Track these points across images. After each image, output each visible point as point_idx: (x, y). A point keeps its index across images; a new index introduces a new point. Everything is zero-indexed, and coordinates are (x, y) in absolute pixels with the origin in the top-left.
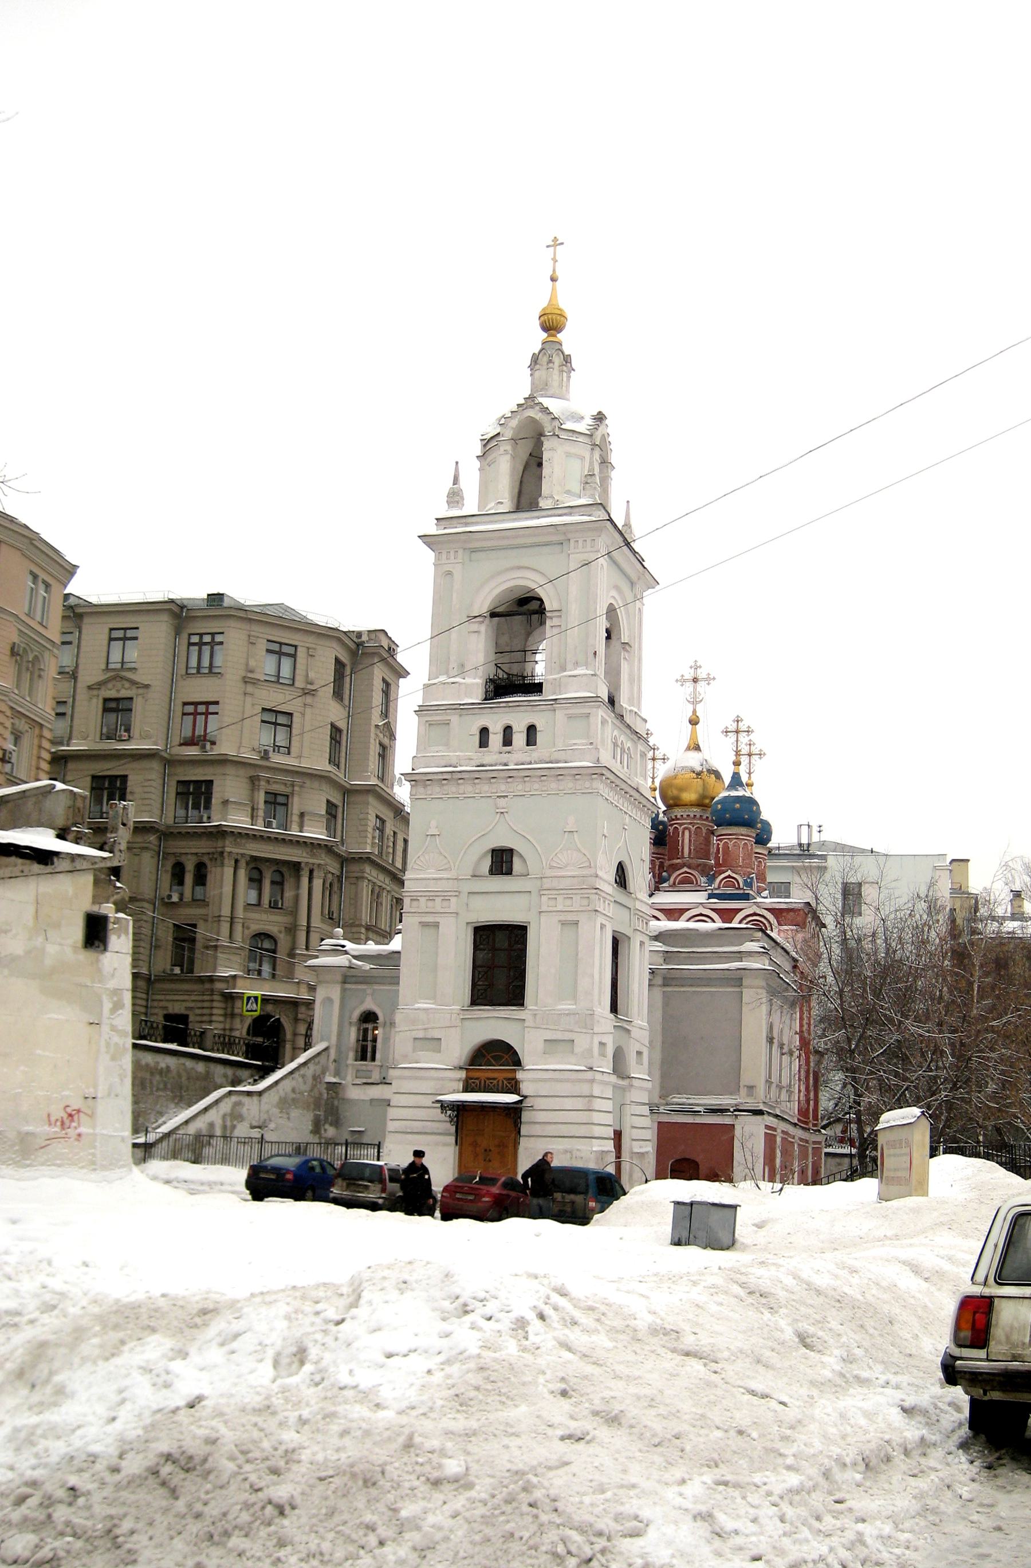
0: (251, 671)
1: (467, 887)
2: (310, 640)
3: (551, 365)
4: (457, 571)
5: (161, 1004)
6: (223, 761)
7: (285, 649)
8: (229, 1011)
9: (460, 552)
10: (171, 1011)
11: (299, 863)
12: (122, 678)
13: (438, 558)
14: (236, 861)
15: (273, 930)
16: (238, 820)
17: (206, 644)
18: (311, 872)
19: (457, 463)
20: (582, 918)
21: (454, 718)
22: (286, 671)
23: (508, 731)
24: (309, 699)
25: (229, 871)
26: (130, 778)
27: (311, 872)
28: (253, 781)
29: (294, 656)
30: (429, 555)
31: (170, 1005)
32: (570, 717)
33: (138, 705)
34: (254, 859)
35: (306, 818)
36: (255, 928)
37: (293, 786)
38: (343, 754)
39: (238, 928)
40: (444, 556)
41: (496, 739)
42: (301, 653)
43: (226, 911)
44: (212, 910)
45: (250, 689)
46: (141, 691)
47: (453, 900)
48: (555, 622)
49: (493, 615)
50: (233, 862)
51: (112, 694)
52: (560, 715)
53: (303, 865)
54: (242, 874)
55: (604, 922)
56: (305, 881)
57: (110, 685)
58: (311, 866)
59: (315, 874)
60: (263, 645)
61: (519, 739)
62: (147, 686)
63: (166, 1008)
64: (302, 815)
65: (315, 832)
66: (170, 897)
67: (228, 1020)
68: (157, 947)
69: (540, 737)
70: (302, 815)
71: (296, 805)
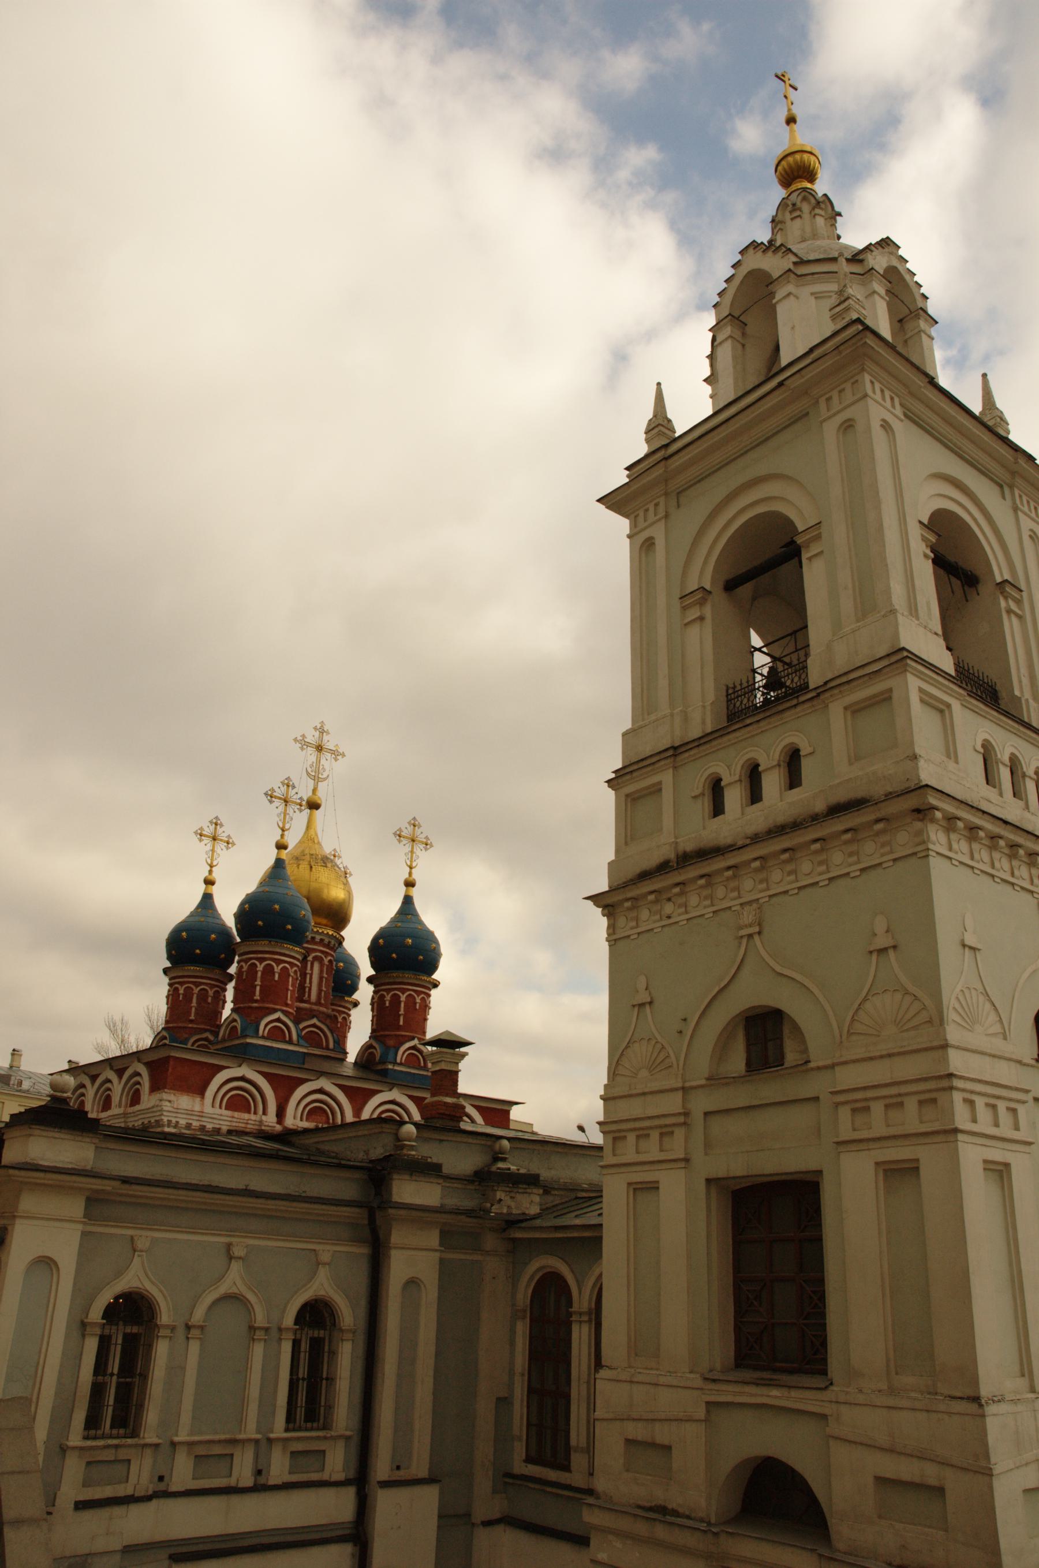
1: (701, 1103)
3: (797, 213)
4: (658, 533)
9: (662, 500)
13: (634, 525)
19: (659, 384)
20: (927, 1156)
21: (667, 778)
23: (754, 775)
30: (621, 525)
32: (855, 710)
40: (641, 518)
41: (734, 797)
47: (679, 1133)
48: (814, 549)
49: (730, 586)
52: (836, 710)
55: (997, 1154)
61: (772, 783)
69: (807, 766)
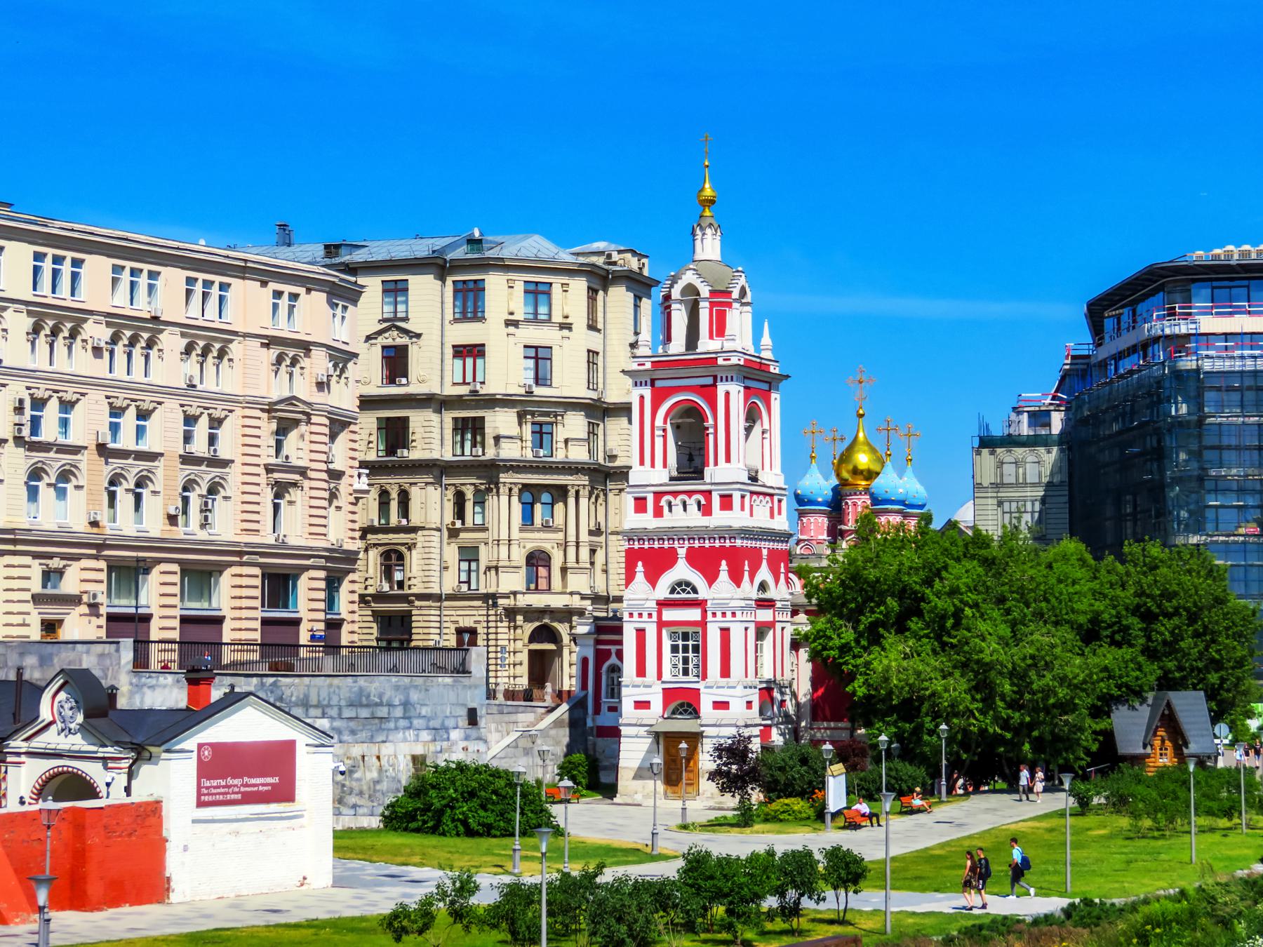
0: (512, 314)
2: (565, 280)
5: (453, 619)
6: (492, 402)
7: (541, 288)
8: (512, 624)
10: (461, 625)
11: (567, 485)
12: (398, 328)
14: (510, 490)
15: (547, 546)
16: (510, 451)
17: (471, 290)
18: (577, 492)
22: (543, 310)
24: (566, 332)
25: (504, 499)
26: (411, 419)
27: (577, 492)
28: (521, 417)
29: (548, 294)
31: (460, 619)
33: (413, 352)
34: (526, 487)
35: (570, 443)
36: (530, 546)
37: (556, 416)
38: (601, 375)
39: (514, 548)
42: (556, 290)
43: (504, 536)
44: (491, 535)
45: (511, 329)
46: (414, 340)
50: (507, 491)
51: (389, 342)
53: (569, 488)
54: (515, 499)
56: (571, 501)
57: (387, 335)
58: (577, 488)
59: (581, 493)
60: (520, 287)
62: (418, 336)
63: (457, 622)
64: (566, 441)
65: (579, 454)
66: (453, 524)
67: (512, 631)
68: (446, 568)
70: (566, 441)
71: (561, 433)
